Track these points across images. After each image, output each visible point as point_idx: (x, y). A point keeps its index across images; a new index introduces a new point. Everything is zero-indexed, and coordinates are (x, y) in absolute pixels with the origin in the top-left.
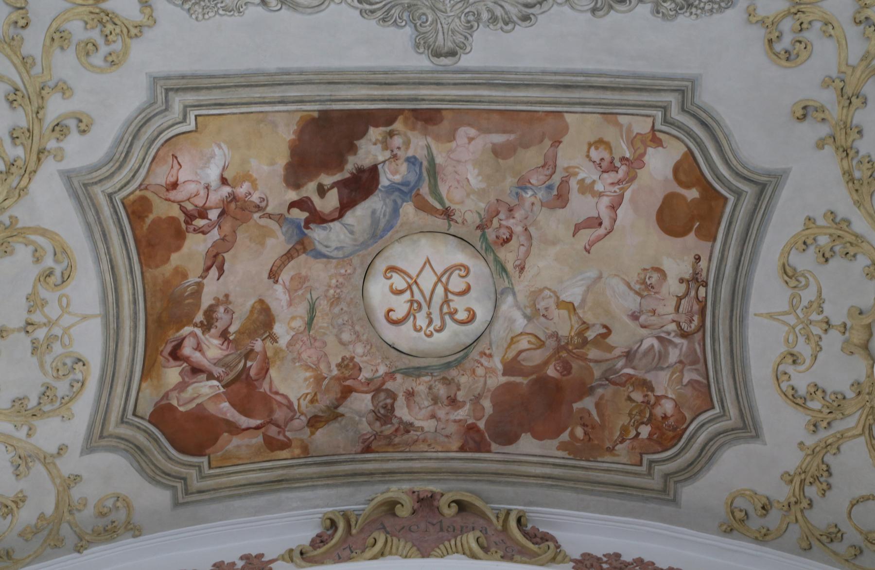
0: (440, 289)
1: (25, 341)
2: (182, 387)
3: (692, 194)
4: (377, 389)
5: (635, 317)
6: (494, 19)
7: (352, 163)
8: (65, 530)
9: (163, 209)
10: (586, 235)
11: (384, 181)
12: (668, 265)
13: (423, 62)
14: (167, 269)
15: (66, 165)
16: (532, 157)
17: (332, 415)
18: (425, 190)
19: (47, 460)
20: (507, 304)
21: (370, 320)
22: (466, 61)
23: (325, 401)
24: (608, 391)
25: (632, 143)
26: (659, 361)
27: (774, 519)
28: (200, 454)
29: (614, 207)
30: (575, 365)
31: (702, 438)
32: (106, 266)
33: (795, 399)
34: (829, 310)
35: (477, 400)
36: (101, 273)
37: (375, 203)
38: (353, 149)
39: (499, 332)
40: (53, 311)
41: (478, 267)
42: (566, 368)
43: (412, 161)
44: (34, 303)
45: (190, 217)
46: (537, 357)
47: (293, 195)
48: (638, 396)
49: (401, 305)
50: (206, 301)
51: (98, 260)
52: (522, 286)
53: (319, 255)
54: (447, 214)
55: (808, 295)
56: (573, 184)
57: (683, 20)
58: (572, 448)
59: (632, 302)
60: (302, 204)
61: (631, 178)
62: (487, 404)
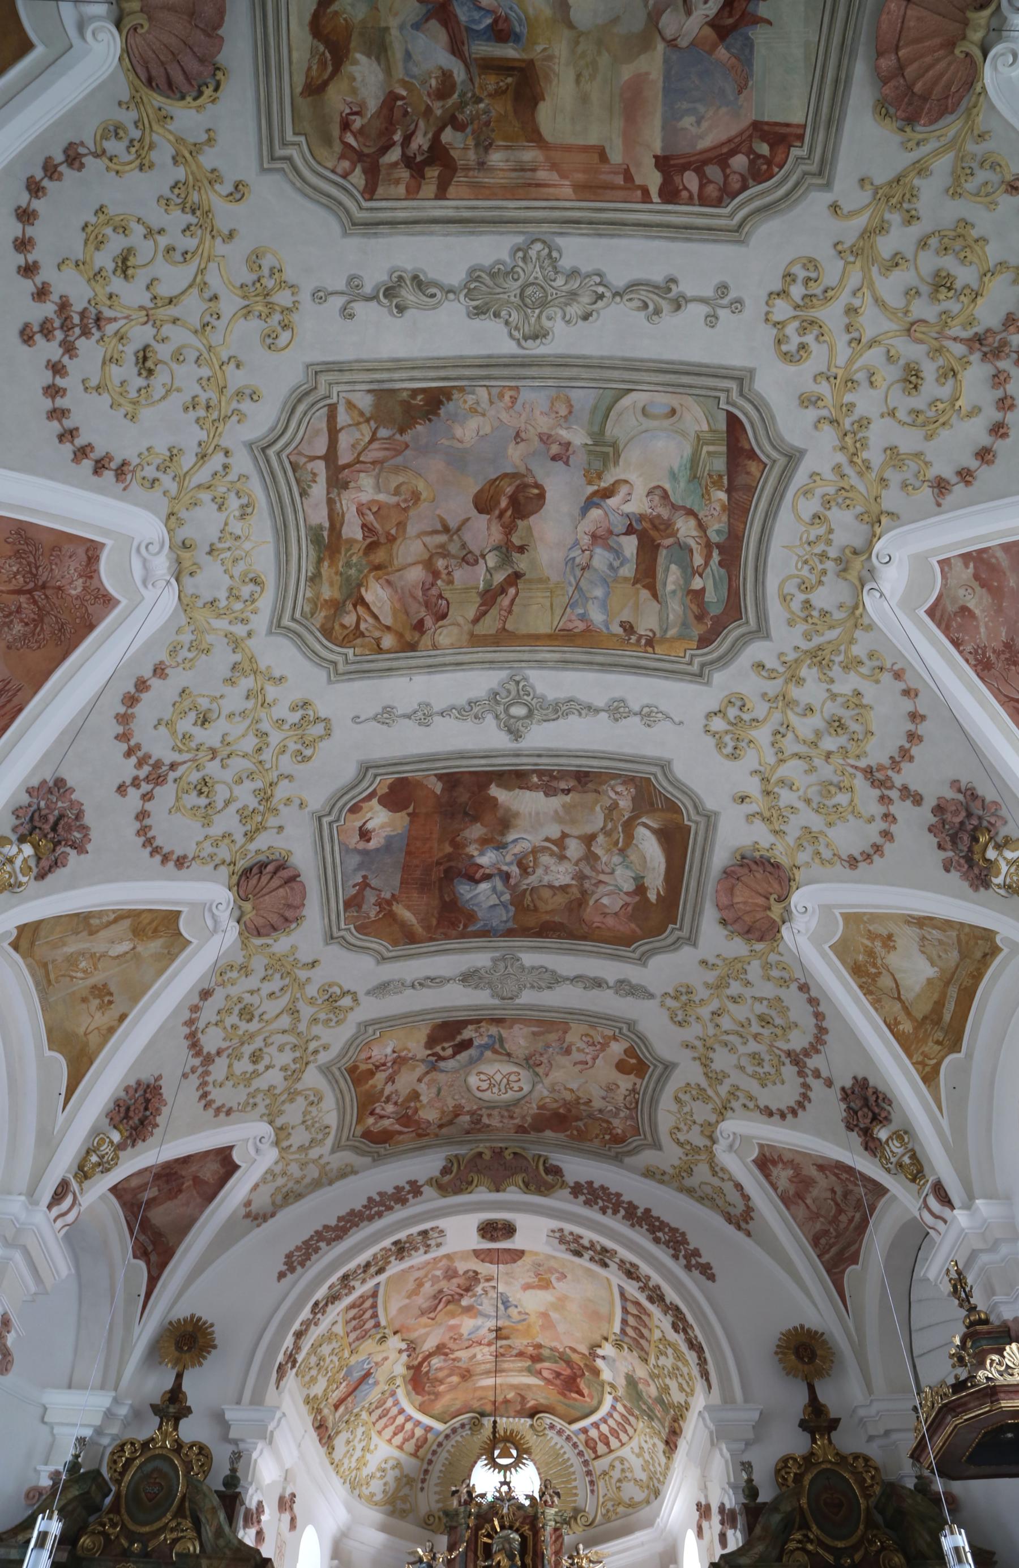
0: (505, 1081)
1: (303, 1127)
2: (376, 1123)
3: (633, 1061)
4: (472, 1113)
5: (604, 1098)
6: (533, 987)
7: (459, 1038)
8: (324, 1180)
9: (363, 1067)
10: (580, 1067)
11: (476, 1043)
12: (620, 1083)
13: (496, 1002)
14: (367, 1086)
15: (320, 1062)
16: (553, 1037)
17: (451, 1123)
18: (497, 1046)
19: (314, 1161)
20: (539, 1086)
21: (469, 1090)
22: (517, 1001)
23: (444, 1120)
24: (590, 1121)
25: (604, 1037)
26: (616, 1115)
27: (666, 1178)
28: (385, 1142)
29: (594, 1059)
30: (574, 1111)
31: (635, 1144)
32: (338, 1091)
33: (679, 1143)
34: (695, 1117)
35: (523, 1117)
36: (335, 1095)
37: (472, 1052)
38: (460, 1033)
39: (535, 1095)
40: (314, 1113)
41: (525, 1074)
42: (569, 1111)
43: (490, 1036)
44: (305, 1114)
45: (377, 1067)
46: (555, 1105)
47: (429, 1052)
48: (605, 1125)
49: (485, 1085)
50: (386, 1093)
51: (334, 1090)
52: (547, 1081)
53: (442, 1071)
54: (509, 1055)
55: (686, 1109)
56: (574, 1048)
57: (630, 999)
58: (571, 1137)
59: (603, 1093)
60: (433, 1055)
61: (603, 1050)
62: (529, 1119)
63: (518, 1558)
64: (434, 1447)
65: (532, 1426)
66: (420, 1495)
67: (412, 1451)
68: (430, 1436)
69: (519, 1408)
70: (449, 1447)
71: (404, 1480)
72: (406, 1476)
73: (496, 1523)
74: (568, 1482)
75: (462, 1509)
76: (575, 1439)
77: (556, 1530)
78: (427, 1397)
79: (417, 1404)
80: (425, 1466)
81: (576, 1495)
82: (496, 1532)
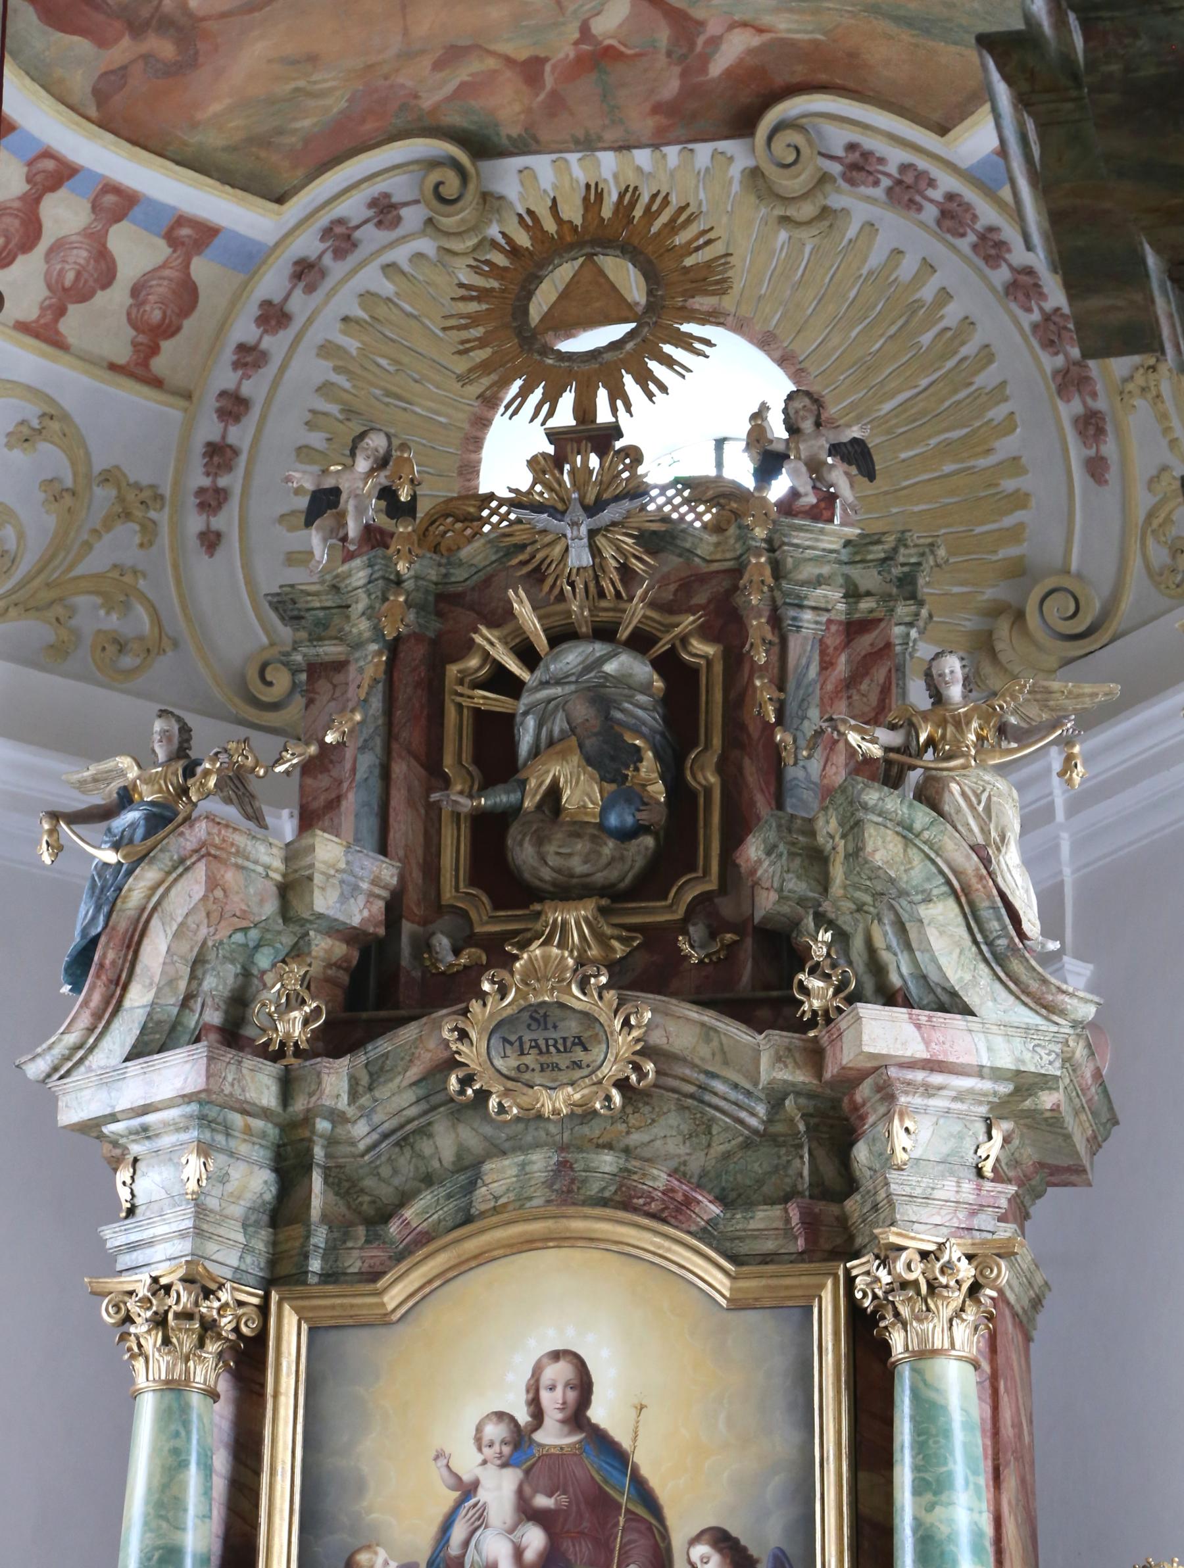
63: (649, 766)
64: (245, 330)
65: (754, 174)
66: (202, 567)
67: (123, 353)
68: (202, 269)
69: (671, 87)
70: (327, 328)
71: (104, 495)
72: (109, 477)
73: (524, 611)
74: (977, 443)
75: (358, 574)
76: (987, 214)
77: (854, 628)
78: (123, 50)
79: (80, 82)
80: (209, 429)
81: (1019, 500)
82: (528, 655)
